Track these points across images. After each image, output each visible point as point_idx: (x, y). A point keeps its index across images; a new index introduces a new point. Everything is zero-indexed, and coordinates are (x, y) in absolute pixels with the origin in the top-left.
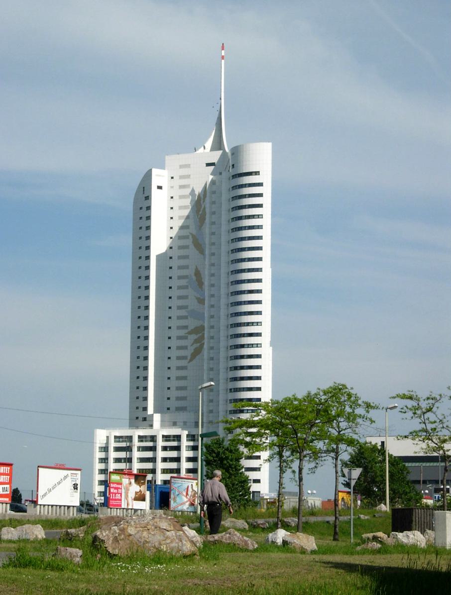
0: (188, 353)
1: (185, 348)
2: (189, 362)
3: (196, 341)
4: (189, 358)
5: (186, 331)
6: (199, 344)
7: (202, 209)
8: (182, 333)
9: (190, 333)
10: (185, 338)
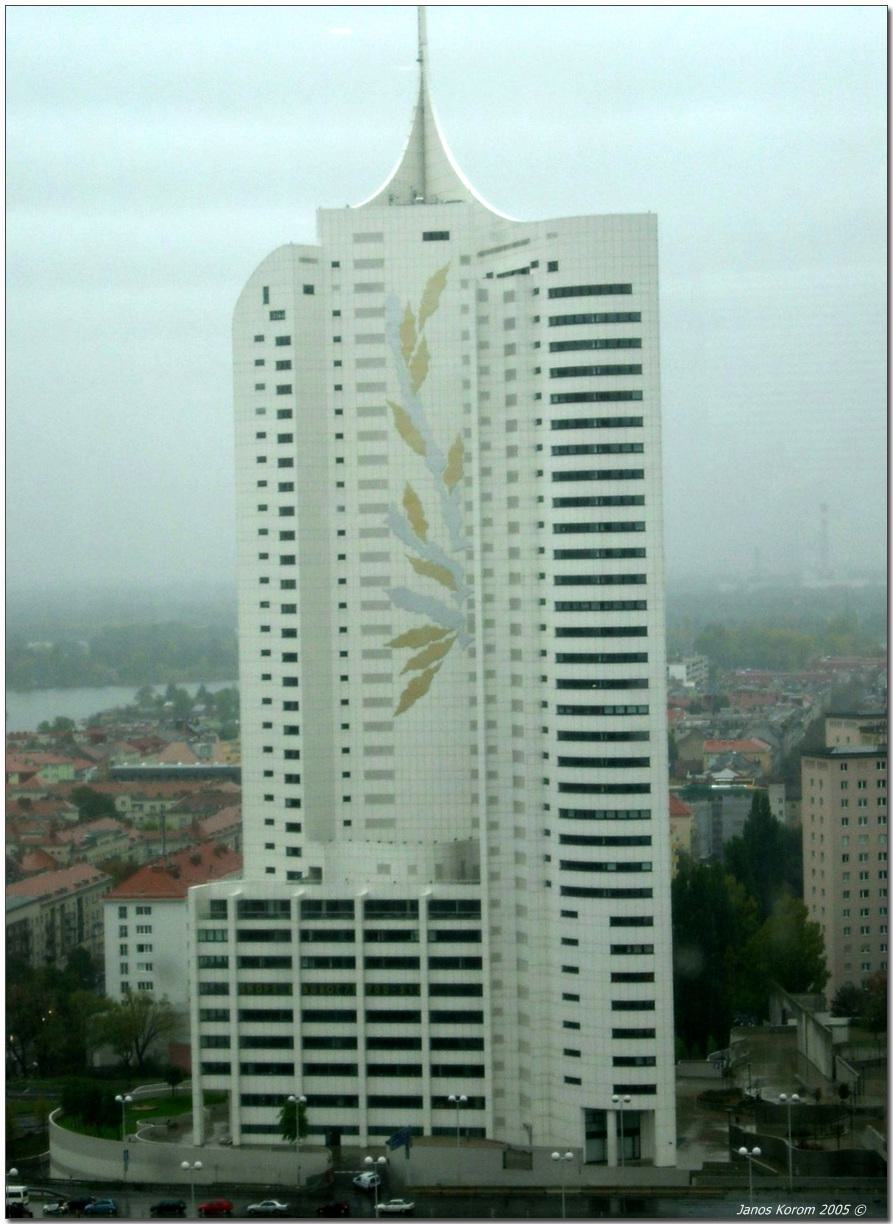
0: (395, 690)
1: (386, 678)
2: (397, 714)
3: (413, 664)
4: (397, 703)
5: (388, 639)
6: (419, 673)
7: (416, 347)
8: (378, 642)
9: (401, 642)
10: (387, 655)
